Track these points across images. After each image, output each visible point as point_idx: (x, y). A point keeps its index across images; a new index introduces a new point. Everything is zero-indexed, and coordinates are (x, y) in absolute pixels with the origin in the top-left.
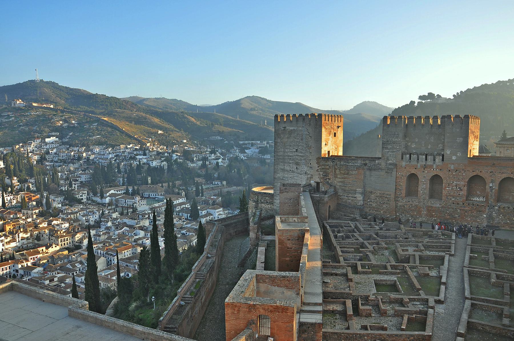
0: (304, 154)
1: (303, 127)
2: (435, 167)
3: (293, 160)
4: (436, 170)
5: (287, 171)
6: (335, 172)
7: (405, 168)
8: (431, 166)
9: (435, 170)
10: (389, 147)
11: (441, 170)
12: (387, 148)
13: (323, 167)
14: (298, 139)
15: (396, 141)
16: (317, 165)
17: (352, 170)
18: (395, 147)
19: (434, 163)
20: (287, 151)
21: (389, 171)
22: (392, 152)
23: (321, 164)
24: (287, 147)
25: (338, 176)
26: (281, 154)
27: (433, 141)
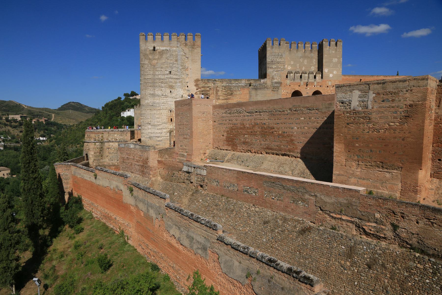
0: (179, 76)
1: (178, 47)
2: (315, 84)
3: (166, 83)
4: (317, 86)
5: (158, 96)
6: (217, 93)
7: (290, 86)
8: (312, 83)
9: (316, 86)
10: (274, 66)
11: (320, 86)
12: (271, 68)
13: (203, 89)
14: (171, 60)
15: (280, 61)
16: (195, 88)
17: (235, 91)
18: (280, 67)
19: (315, 81)
20: (157, 73)
21: (274, 89)
22: (277, 71)
23: (201, 86)
24: (158, 69)
25: (221, 98)
26: (150, 77)
27: (306, 64)
